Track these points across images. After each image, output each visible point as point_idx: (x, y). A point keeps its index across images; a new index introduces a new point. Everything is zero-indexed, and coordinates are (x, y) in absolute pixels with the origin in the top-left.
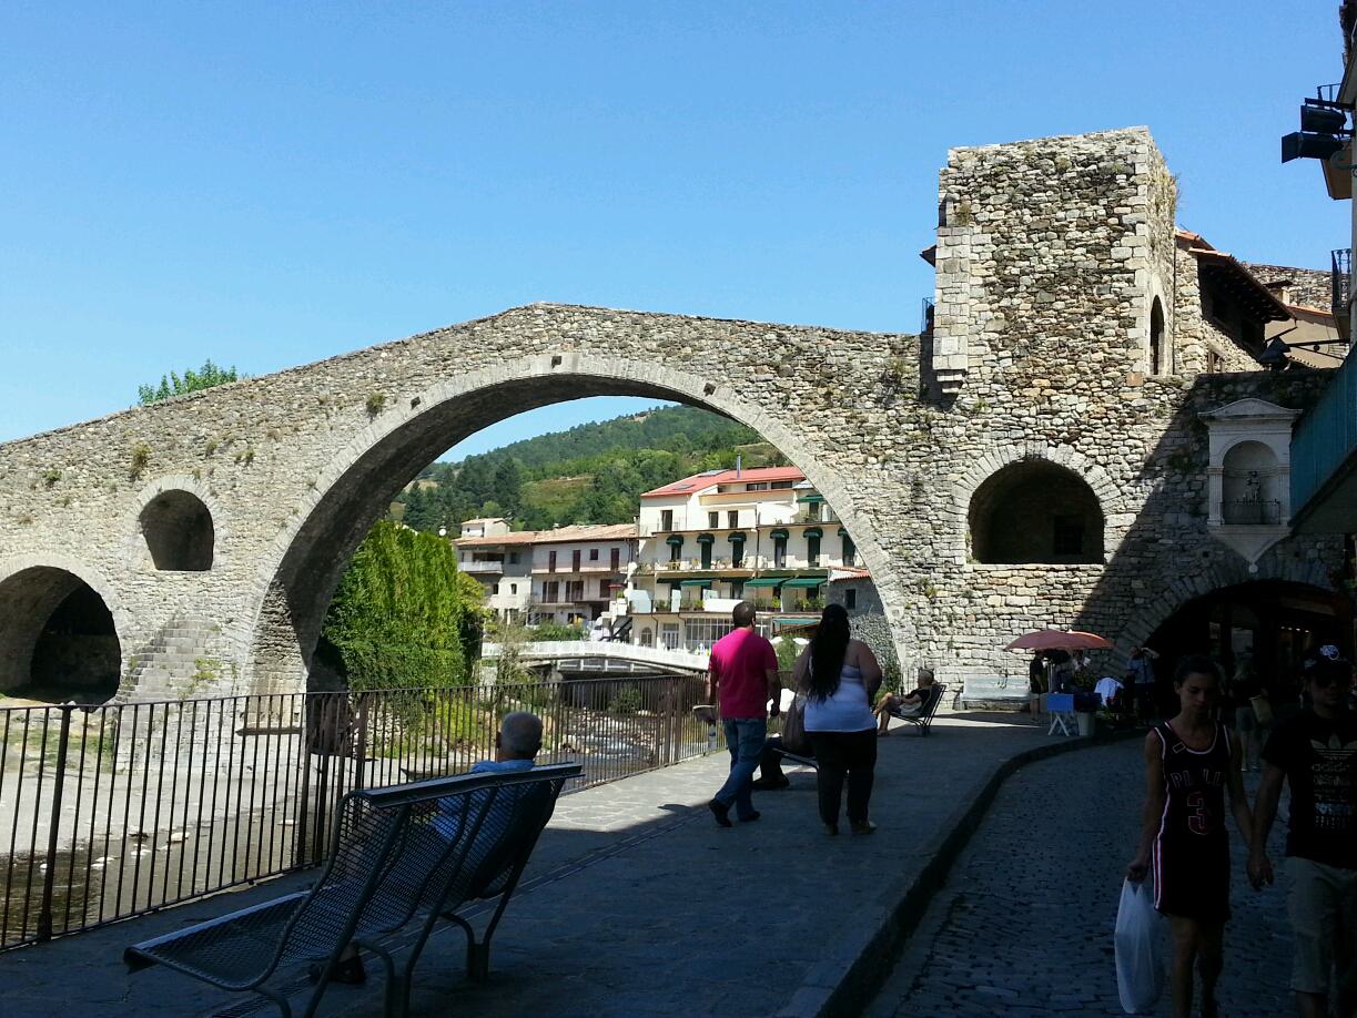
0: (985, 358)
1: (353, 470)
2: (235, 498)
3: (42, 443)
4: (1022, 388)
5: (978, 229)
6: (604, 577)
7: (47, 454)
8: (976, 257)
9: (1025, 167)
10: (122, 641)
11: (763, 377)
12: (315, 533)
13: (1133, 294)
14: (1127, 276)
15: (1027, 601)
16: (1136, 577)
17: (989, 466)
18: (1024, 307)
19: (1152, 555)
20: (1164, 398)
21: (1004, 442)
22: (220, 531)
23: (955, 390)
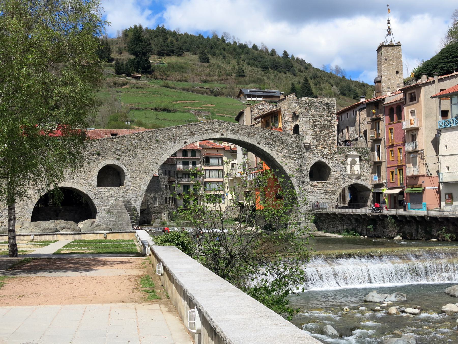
2: (132, 166)
5: (310, 114)
9: (317, 103)
10: (97, 208)
15: (320, 188)
17: (312, 162)
22: (128, 176)
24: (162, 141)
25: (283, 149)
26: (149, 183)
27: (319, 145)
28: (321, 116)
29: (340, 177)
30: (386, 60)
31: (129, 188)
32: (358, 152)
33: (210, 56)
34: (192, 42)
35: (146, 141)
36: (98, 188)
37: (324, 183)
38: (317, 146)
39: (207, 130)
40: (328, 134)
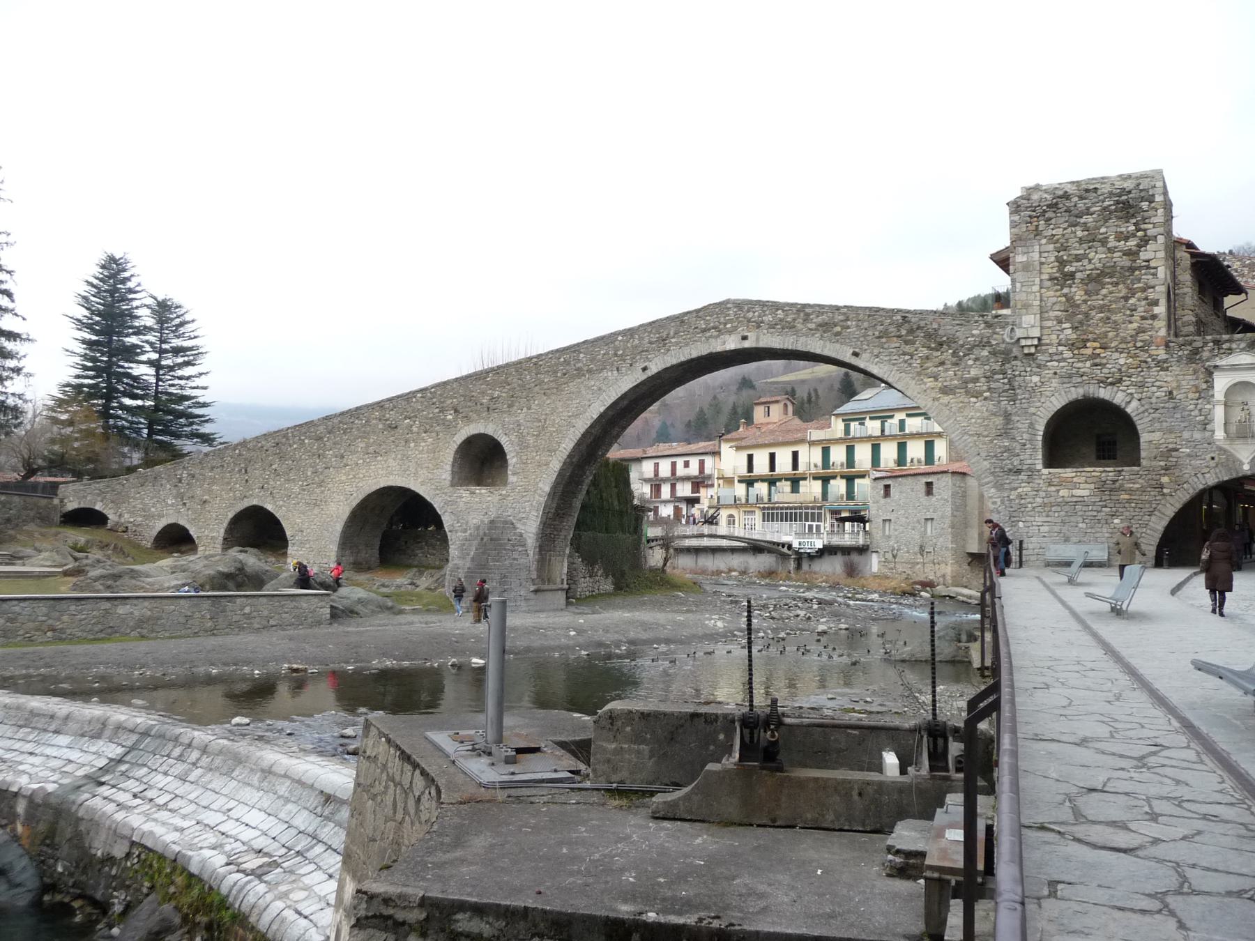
0: (1052, 329)
1: (602, 416)
2: (521, 438)
4: (1080, 348)
5: (1044, 241)
6: (694, 480)
7: (391, 413)
8: (1043, 260)
9: (1076, 199)
10: (449, 534)
11: (893, 345)
12: (574, 460)
13: (1157, 283)
14: (1152, 271)
15: (1086, 493)
16: (1165, 475)
17: (1057, 402)
18: (1078, 294)
19: (1176, 460)
20: (1180, 353)
21: (1068, 385)
22: (512, 459)
23: (1033, 350)
24: (590, 371)
25: (942, 363)
26: (555, 476)
28: (1094, 240)
29: (1177, 450)
35: (556, 372)
36: (451, 489)
37: (1107, 472)
39: (704, 331)
40: (1126, 299)
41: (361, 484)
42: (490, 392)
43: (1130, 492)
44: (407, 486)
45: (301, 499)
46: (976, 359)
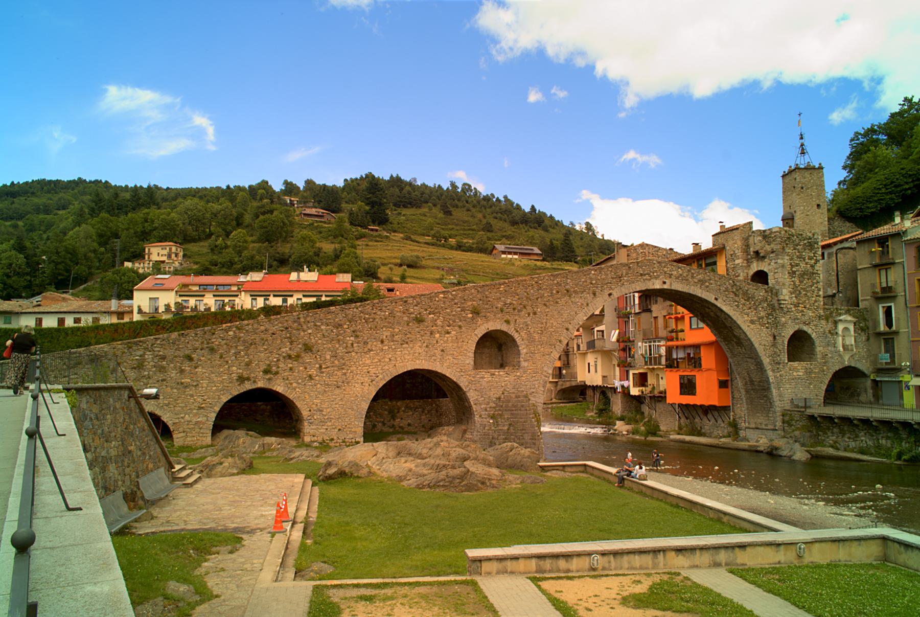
2: (529, 334)
3: (410, 300)
7: (415, 308)
10: (474, 407)
15: (801, 374)
17: (791, 332)
24: (575, 292)
25: (750, 308)
27: (799, 303)
30: (802, 188)
31: (525, 372)
32: (850, 315)
33: (452, 209)
34: (431, 193)
35: (551, 290)
36: (474, 372)
38: (796, 305)
39: (641, 275)
40: (811, 286)
41: (387, 367)
42: (503, 299)
43: (815, 372)
44: (434, 369)
45: (319, 381)
46: (762, 308)
